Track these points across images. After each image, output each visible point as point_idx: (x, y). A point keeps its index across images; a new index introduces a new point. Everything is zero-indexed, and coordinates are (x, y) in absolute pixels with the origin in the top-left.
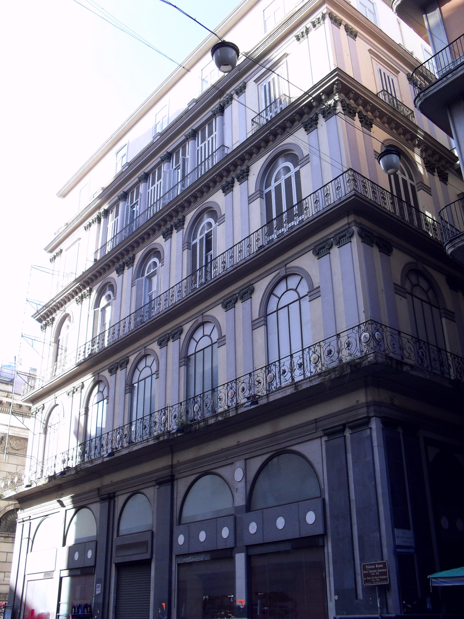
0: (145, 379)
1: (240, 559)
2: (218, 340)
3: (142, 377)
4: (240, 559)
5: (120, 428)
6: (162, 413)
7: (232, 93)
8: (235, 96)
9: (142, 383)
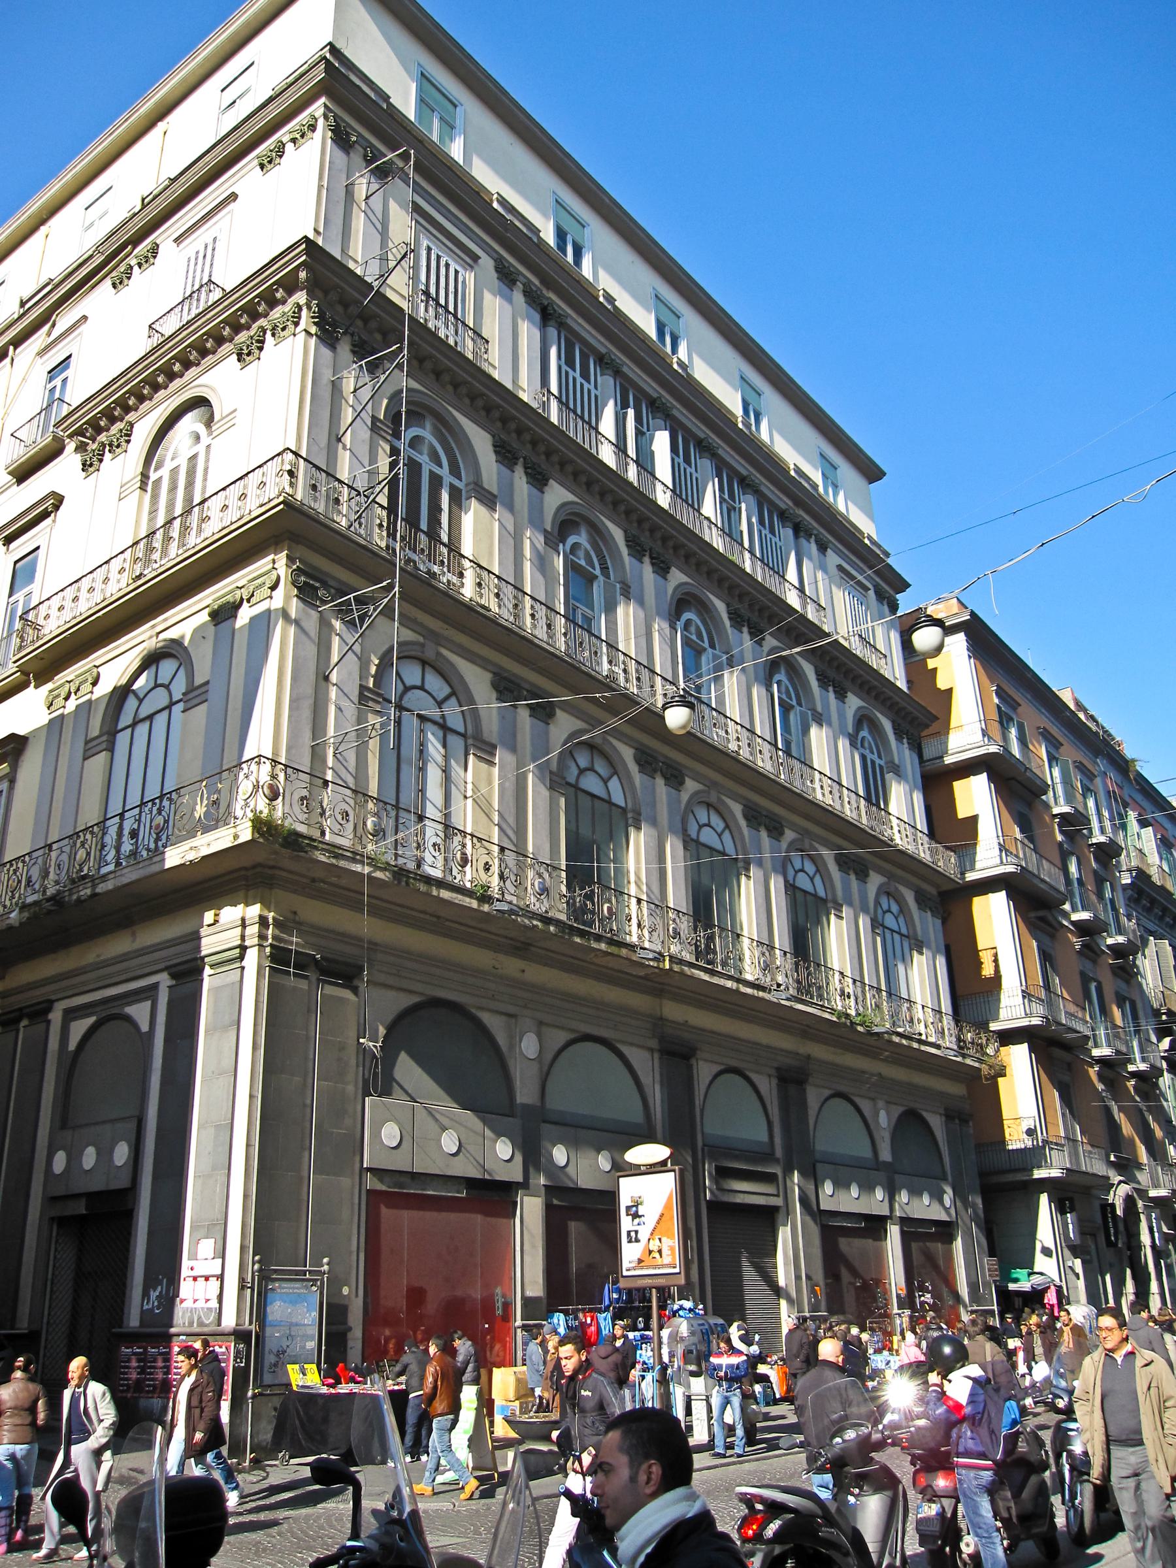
0: (150, 717)
1: (894, 1231)
2: (184, 694)
3: (144, 712)
4: (894, 1231)
5: (87, 829)
6: (155, 809)
7: (285, 140)
8: (289, 147)
9: (143, 729)
